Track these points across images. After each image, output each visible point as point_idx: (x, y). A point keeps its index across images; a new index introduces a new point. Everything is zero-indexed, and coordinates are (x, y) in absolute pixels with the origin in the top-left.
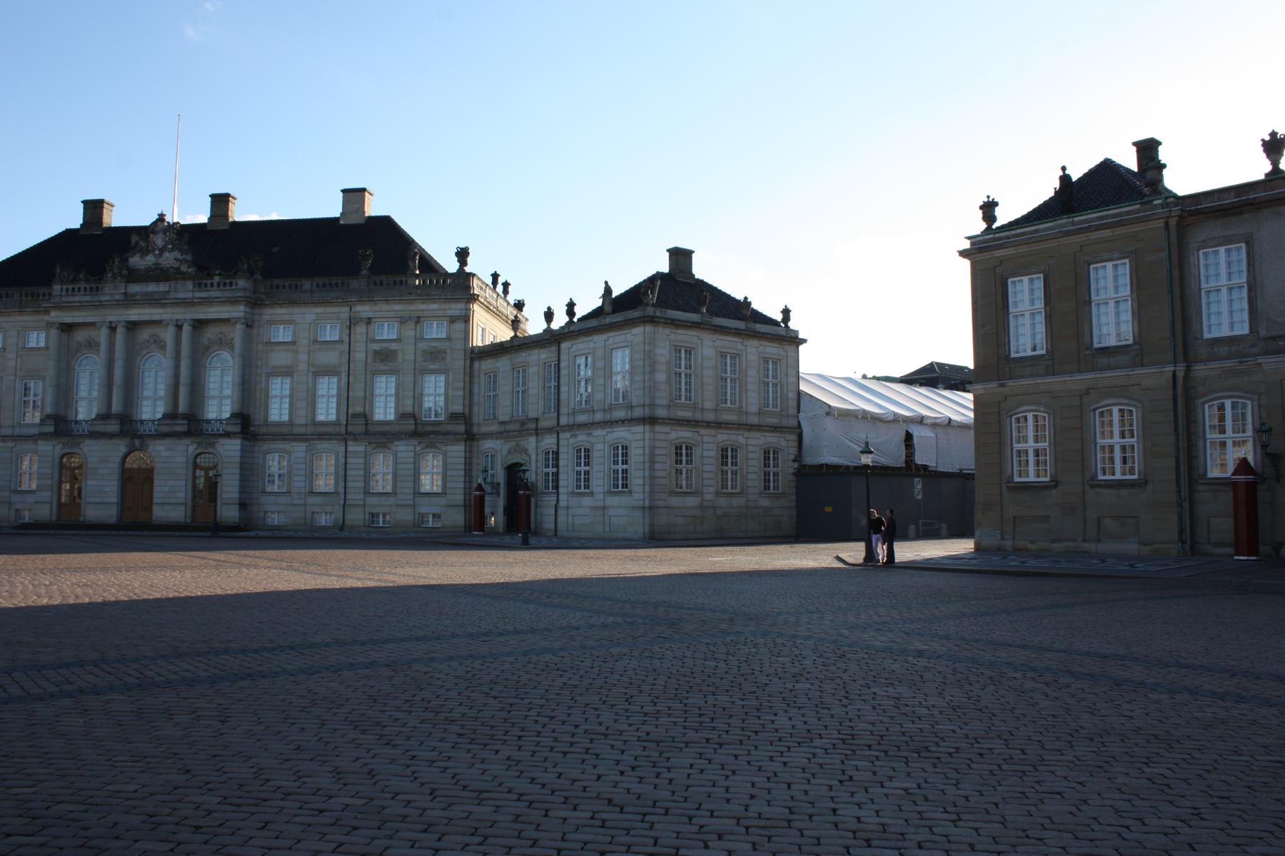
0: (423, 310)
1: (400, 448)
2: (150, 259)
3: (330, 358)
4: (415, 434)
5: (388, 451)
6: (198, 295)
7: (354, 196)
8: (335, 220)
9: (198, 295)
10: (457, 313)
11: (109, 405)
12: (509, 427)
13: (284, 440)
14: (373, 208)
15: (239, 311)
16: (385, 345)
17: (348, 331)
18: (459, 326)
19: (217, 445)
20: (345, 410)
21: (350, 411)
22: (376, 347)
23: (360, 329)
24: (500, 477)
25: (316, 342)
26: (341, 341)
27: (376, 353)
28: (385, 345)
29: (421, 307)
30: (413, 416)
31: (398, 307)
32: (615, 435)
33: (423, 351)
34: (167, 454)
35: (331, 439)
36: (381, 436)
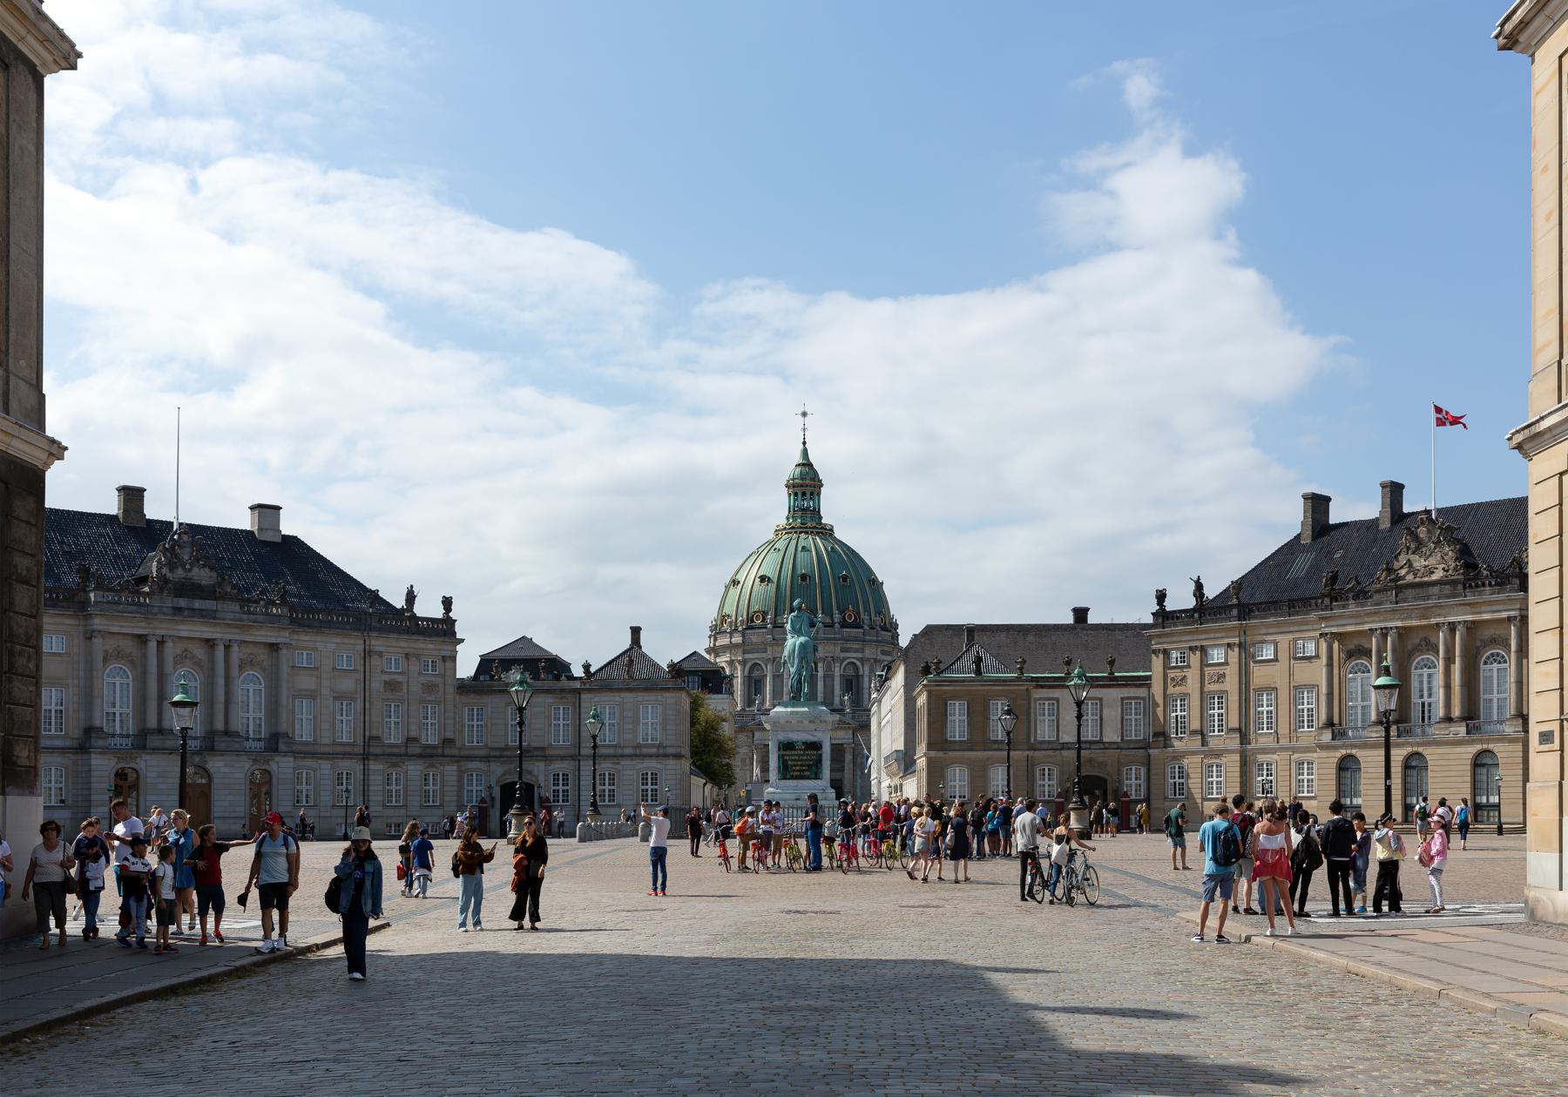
0: (423, 649)
1: (410, 767)
3: (348, 684)
4: (420, 756)
5: (400, 769)
10: (447, 653)
11: (144, 720)
13: (312, 758)
16: (393, 677)
17: (362, 662)
19: (271, 763)
20: (362, 731)
21: (367, 733)
22: (387, 678)
23: (375, 661)
24: (497, 792)
25: (334, 669)
27: (386, 682)
28: (393, 677)
29: (422, 646)
30: (416, 740)
31: (403, 644)
32: (645, 765)
33: (423, 684)
34: (227, 770)
35: (351, 759)
36: (397, 756)
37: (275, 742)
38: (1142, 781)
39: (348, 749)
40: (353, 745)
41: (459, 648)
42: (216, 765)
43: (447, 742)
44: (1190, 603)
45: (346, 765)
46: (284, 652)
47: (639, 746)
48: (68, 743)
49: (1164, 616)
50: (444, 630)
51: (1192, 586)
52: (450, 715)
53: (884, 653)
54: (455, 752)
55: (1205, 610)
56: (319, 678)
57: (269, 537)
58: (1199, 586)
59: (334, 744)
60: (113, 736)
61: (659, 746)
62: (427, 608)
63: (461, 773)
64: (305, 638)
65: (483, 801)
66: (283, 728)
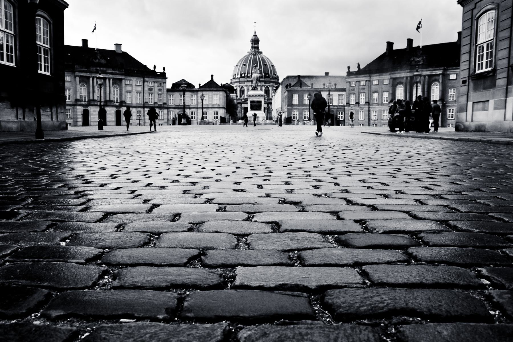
2: (97, 60)
3: (139, 89)
6: (113, 72)
7: (118, 45)
8: (114, 51)
9: (113, 72)
12: (180, 107)
14: (124, 49)
15: (123, 77)
18: (165, 84)
22: (149, 87)
24: (177, 116)
26: (141, 85)
37: (122, 103)
38: (343, 115)
39: (140, 105)
40: (141, 104)
41: (167, 80)
42: (108, 109)
43: (165, 104)
44: (356, 69)
45: (139, 109)
46: (123, 81)
47: (213, 105)
48: (71, 103)
49: (350, 74)
50: (163, 76)
51: (357, 65)
52: (165, 97)
53: (275, 84)
54: (166, 106)
55: (360, 72)
56: (132, 87)
57: (119, 52)
58: (359, 65)
59: (136, 104)
60: (82, 101)
61: (219, 105)
62: (159, 70)
63: (168, 112)
64: (129, 78)
65: (174, 118)
66: (123, 99)
